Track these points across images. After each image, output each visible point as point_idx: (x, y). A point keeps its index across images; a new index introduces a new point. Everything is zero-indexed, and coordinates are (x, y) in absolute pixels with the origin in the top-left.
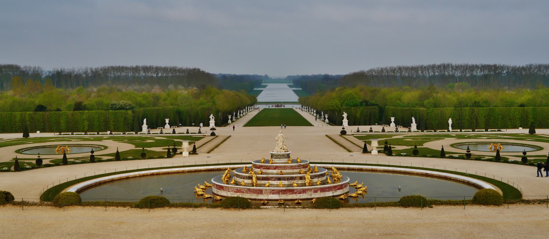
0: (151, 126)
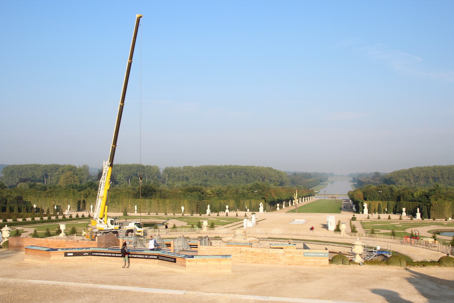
0: (213, 210)
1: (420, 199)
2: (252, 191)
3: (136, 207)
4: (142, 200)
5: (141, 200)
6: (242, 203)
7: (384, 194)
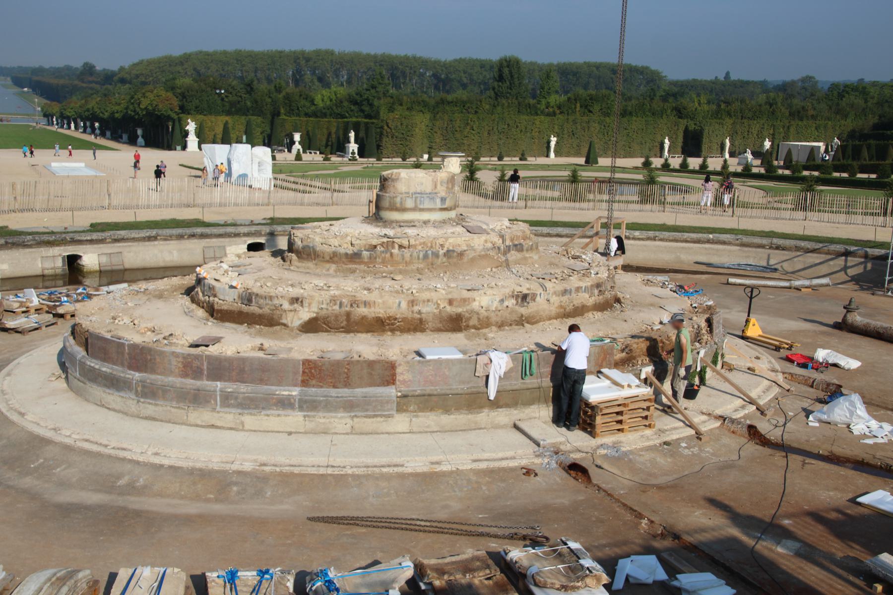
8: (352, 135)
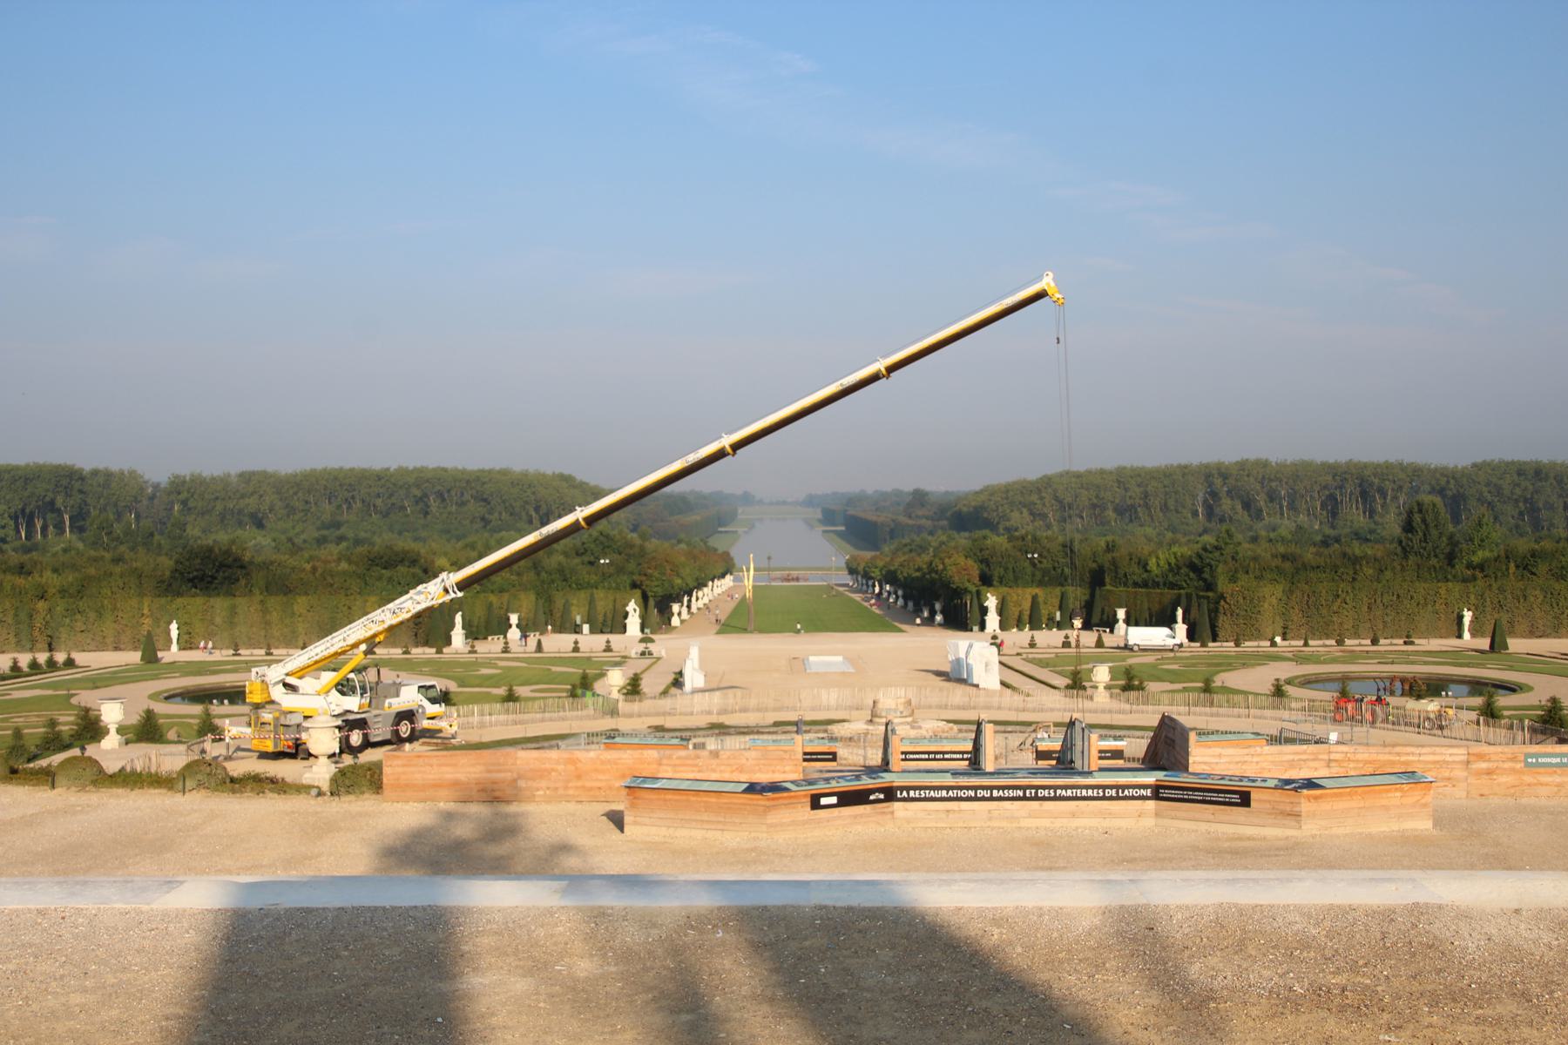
1: (1171, 578)
2: (586, 558)
3: (174, 627)
4: (199, 601)
5: (195, 603)
6: (559, 603)
7: (1046, 564)
8: (1180, 612)
